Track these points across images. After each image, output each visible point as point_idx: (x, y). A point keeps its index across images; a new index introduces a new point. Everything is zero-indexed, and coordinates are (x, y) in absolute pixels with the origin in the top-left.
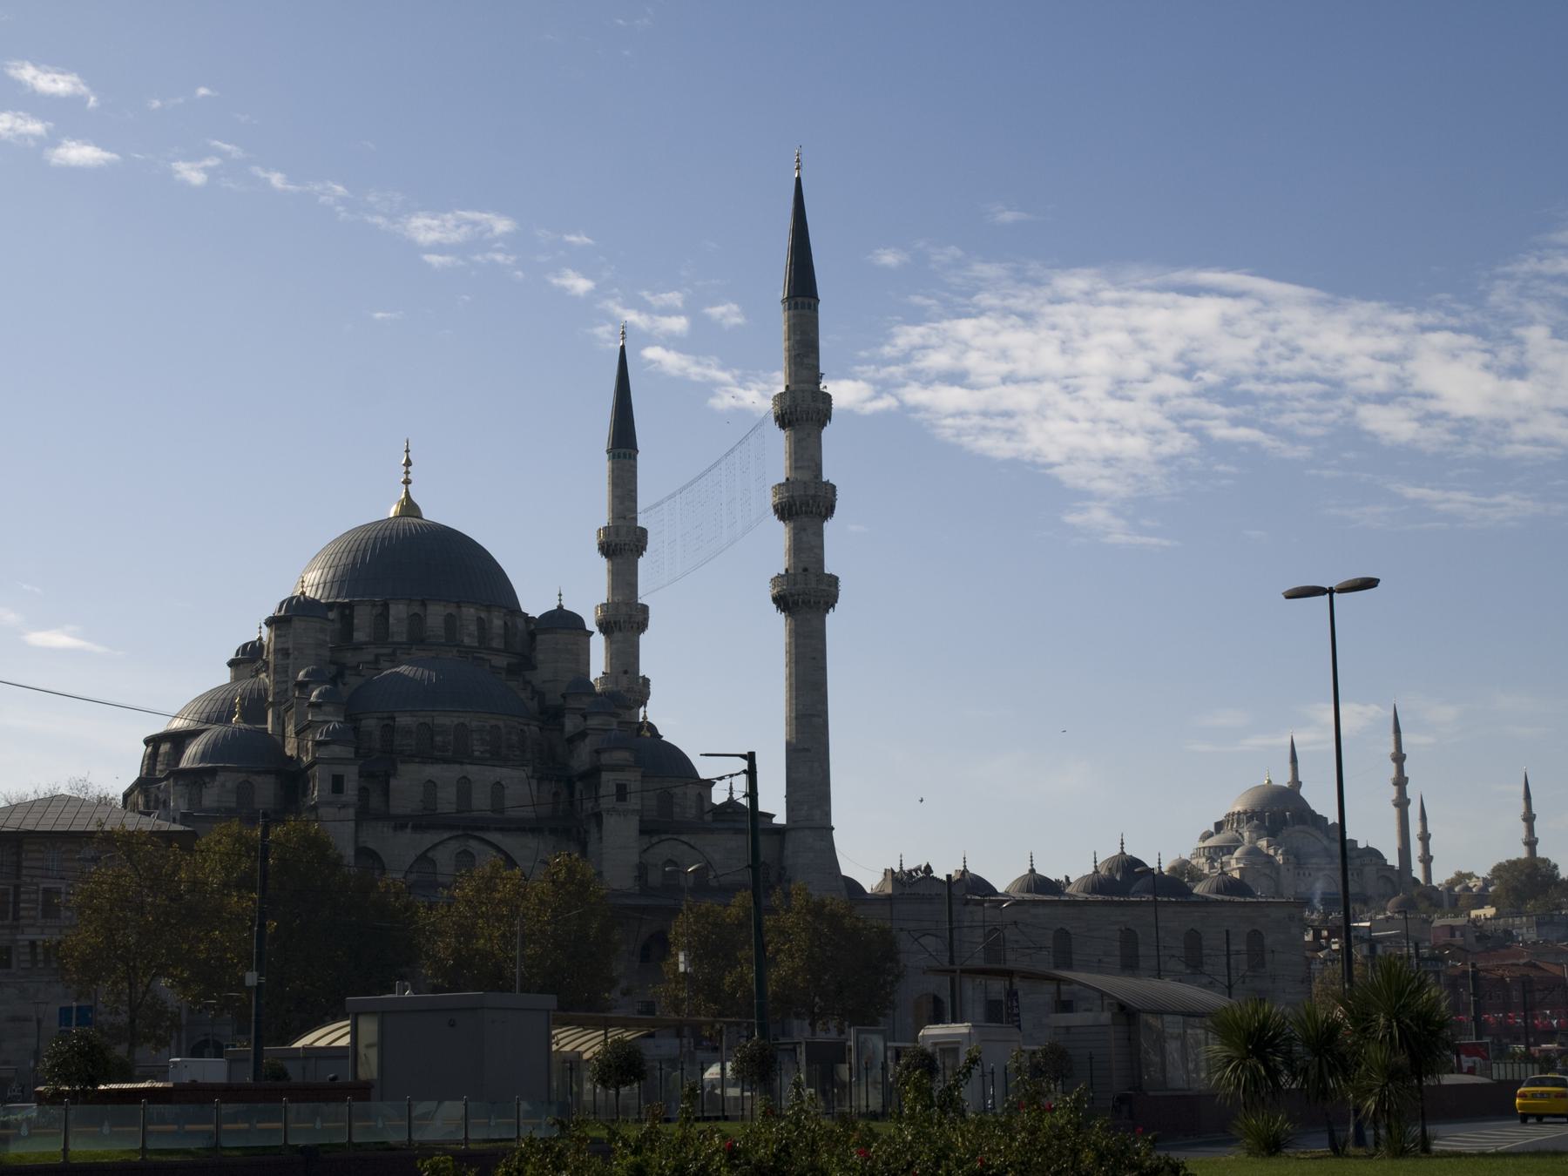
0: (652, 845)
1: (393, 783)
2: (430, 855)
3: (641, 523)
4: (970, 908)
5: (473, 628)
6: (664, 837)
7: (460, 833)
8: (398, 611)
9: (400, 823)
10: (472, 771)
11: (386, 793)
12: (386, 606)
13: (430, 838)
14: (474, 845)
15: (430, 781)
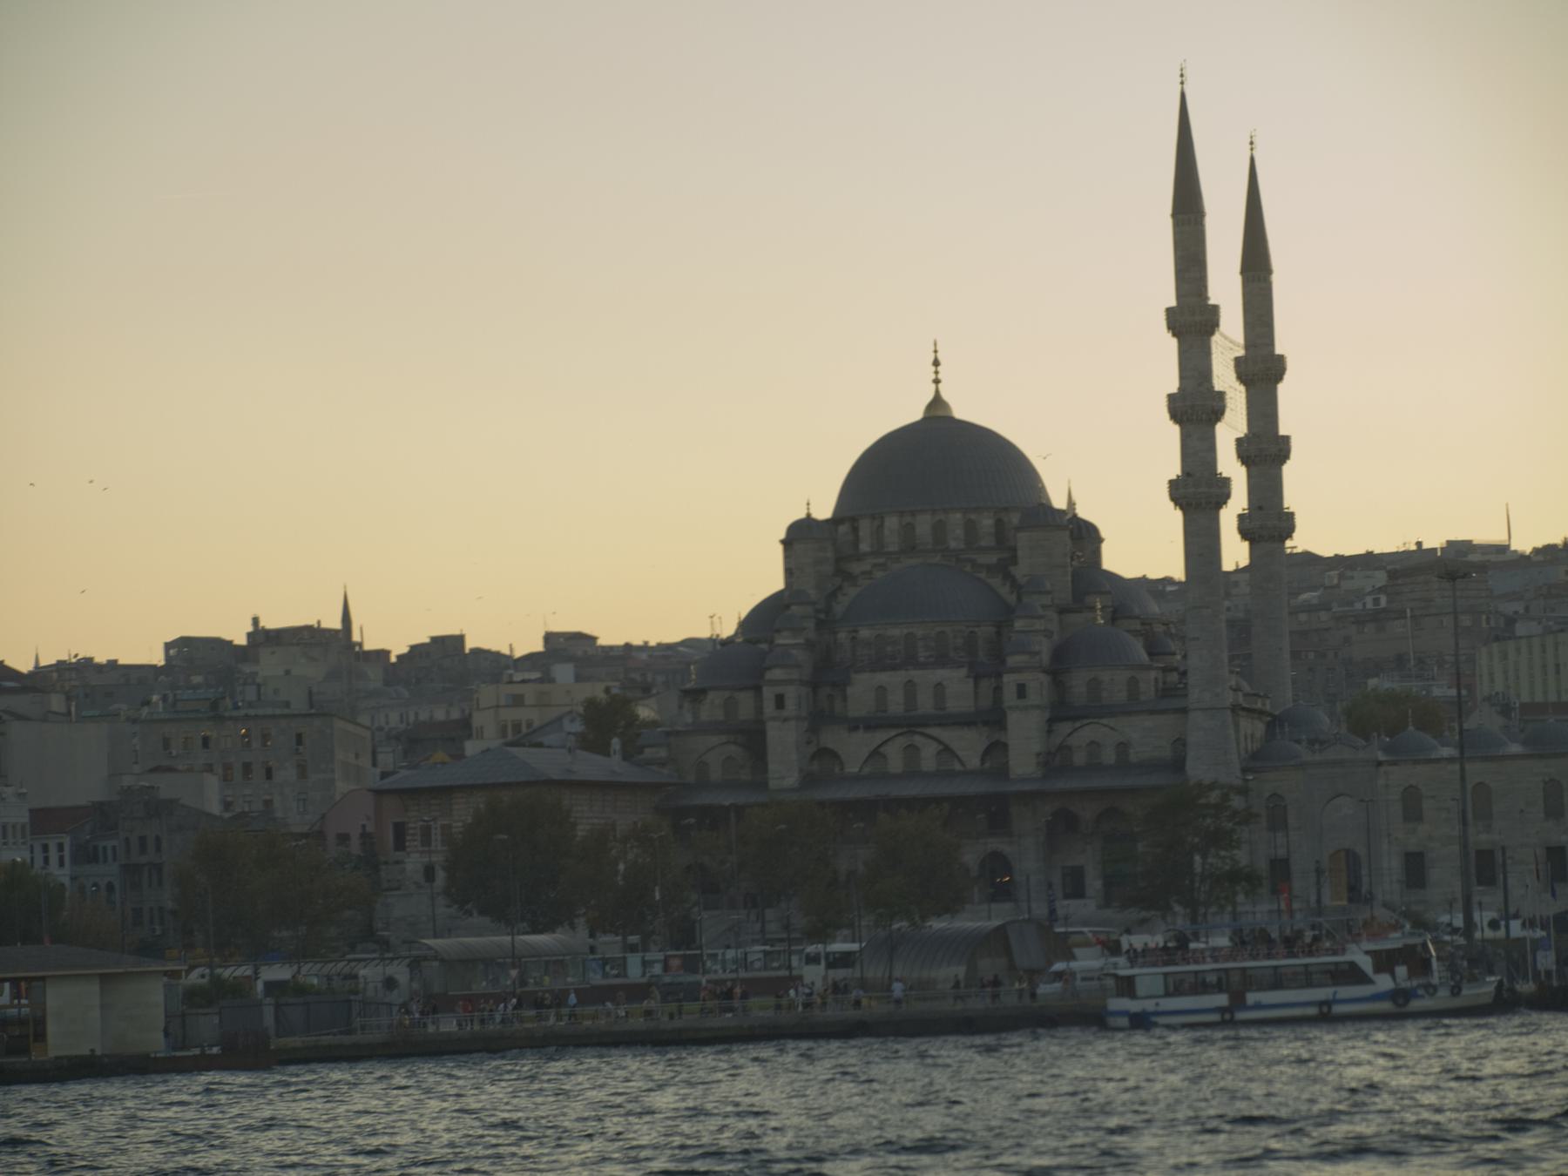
0: (1076, 730)
1: (849, 690)
2: (882, 750)
3: (1278, 350)
4: (1383, 769)
5: (960, 532)
6: (1086, 721)
7: (905, 730)
8: (892, 523)
9: (854, 725)
10: (915, 674)
11: (845, 699)
12: (882, 518)
13: (880, 736)
14: (918, 739)
15: (881, 687)
